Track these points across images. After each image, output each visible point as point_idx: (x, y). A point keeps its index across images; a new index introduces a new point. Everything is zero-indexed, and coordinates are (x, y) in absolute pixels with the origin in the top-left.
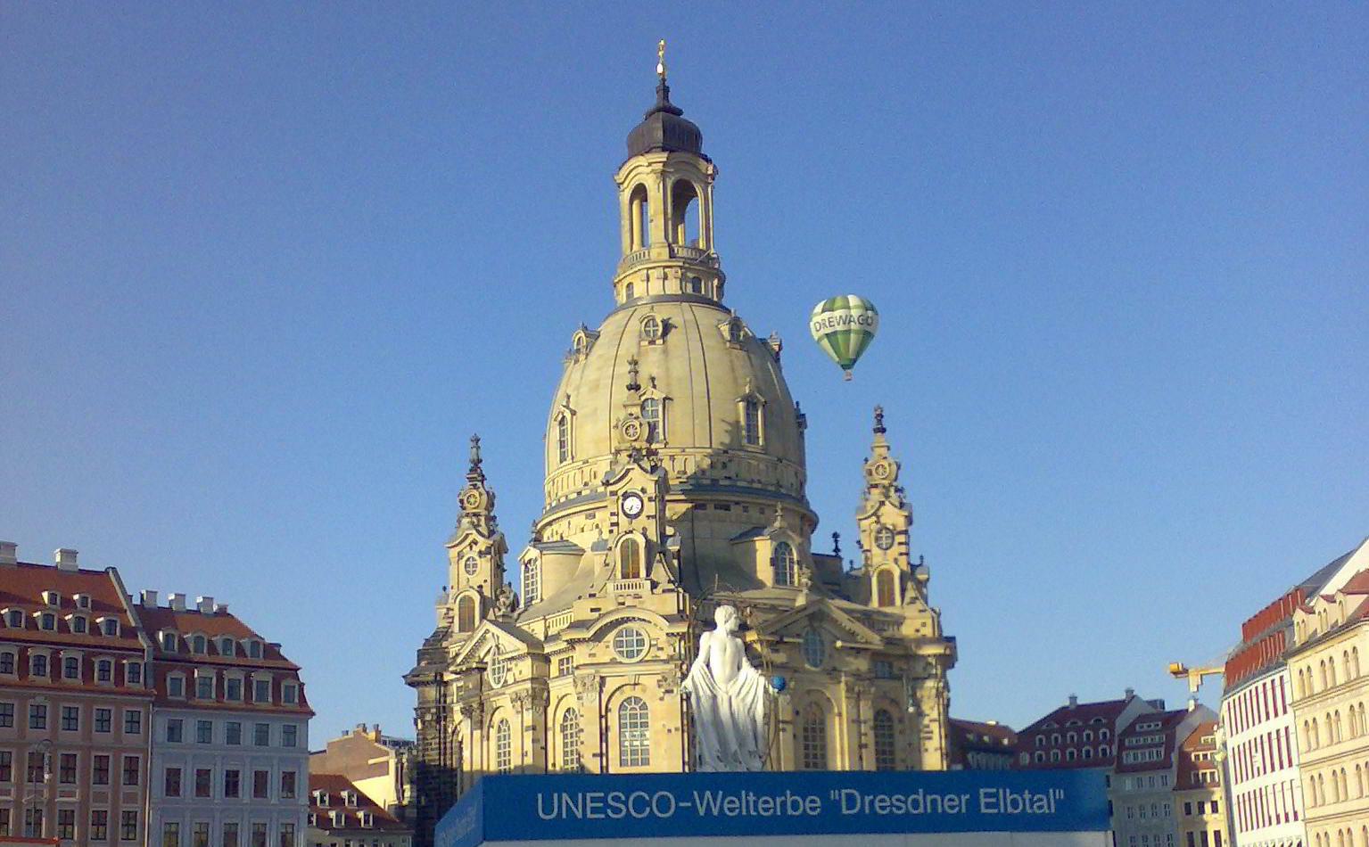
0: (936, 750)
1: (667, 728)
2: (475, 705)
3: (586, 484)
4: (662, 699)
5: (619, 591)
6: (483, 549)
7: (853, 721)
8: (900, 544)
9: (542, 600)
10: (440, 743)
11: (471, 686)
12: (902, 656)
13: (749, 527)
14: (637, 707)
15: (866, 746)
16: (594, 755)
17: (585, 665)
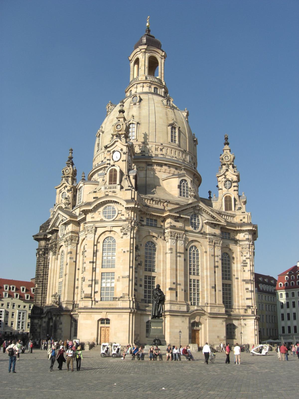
0: (248, 271)
1: (124, 250)
2: (54, 246)
3: (105, 158)
4: (122, 238)
5: (107, 190)
6: (69, 188)
7: (212, 255)
8: (234, 186)
9: (83, 202)
10: (44, 263)
11: (53, 238)
12: (234, 230)
13: (171, 175)
14: (111, 241)
15: (218, 267)
16: (90, 262)
17: (89, 222)
